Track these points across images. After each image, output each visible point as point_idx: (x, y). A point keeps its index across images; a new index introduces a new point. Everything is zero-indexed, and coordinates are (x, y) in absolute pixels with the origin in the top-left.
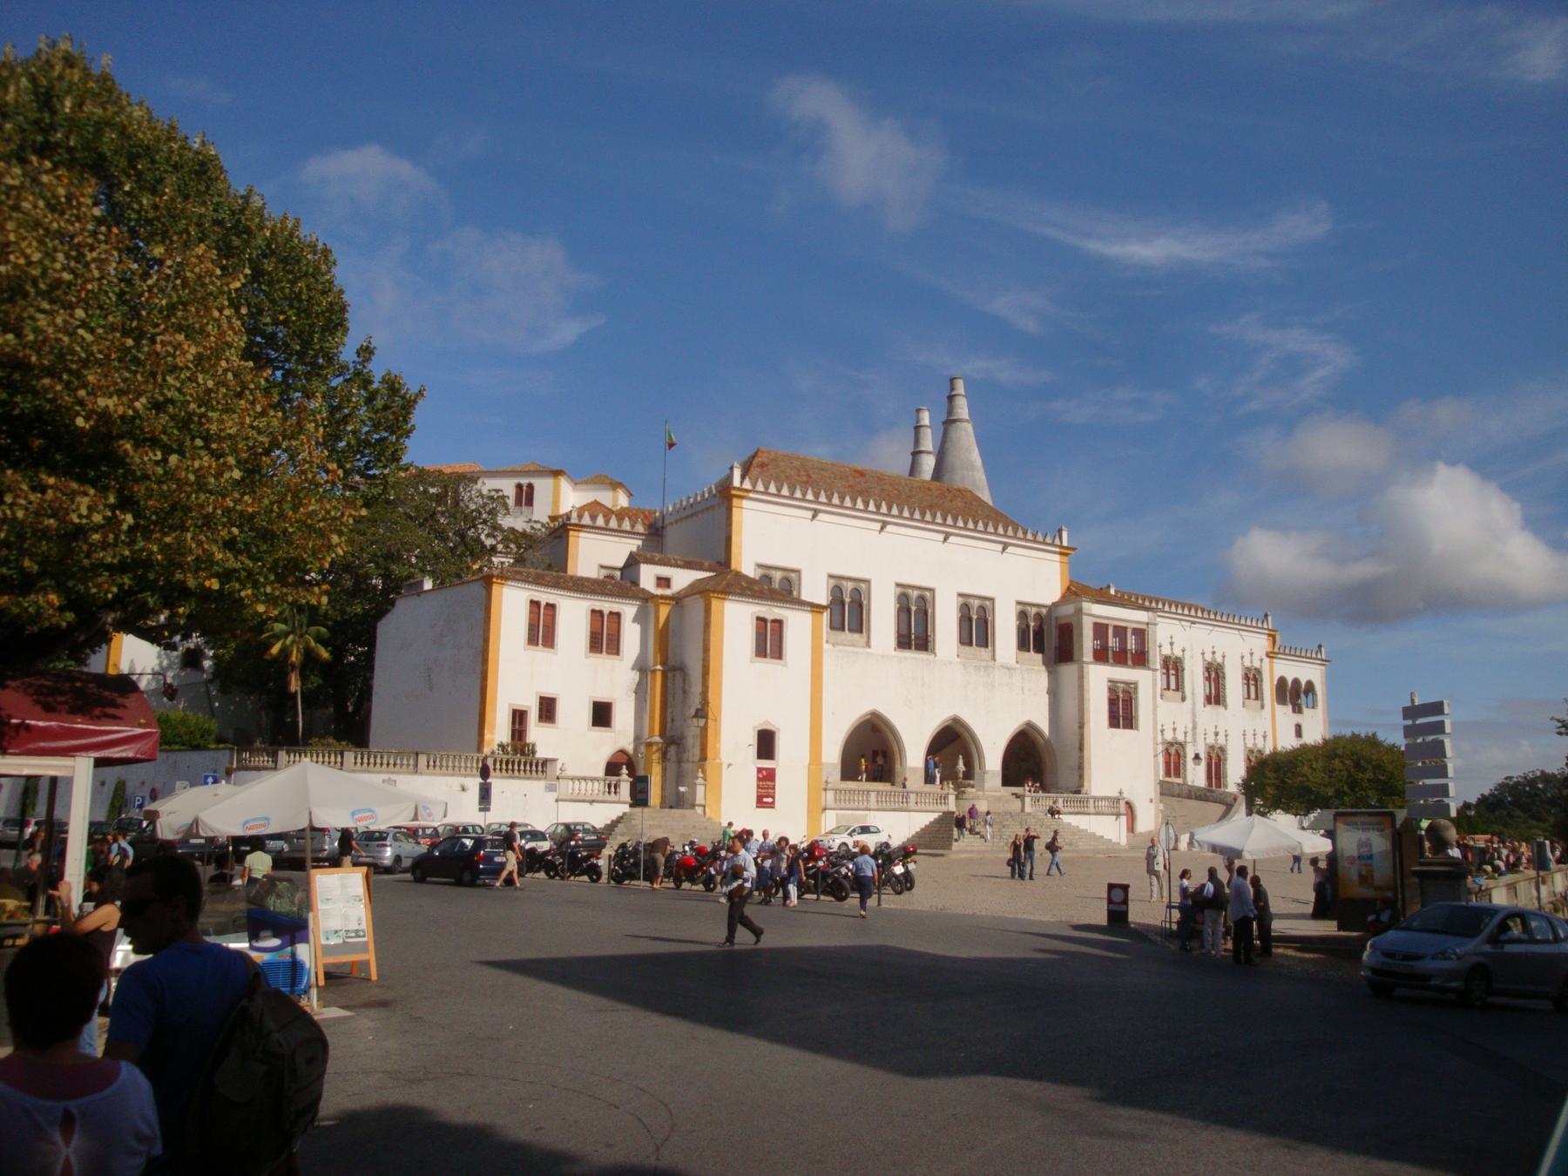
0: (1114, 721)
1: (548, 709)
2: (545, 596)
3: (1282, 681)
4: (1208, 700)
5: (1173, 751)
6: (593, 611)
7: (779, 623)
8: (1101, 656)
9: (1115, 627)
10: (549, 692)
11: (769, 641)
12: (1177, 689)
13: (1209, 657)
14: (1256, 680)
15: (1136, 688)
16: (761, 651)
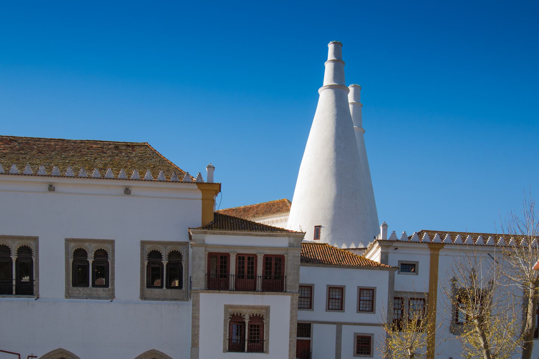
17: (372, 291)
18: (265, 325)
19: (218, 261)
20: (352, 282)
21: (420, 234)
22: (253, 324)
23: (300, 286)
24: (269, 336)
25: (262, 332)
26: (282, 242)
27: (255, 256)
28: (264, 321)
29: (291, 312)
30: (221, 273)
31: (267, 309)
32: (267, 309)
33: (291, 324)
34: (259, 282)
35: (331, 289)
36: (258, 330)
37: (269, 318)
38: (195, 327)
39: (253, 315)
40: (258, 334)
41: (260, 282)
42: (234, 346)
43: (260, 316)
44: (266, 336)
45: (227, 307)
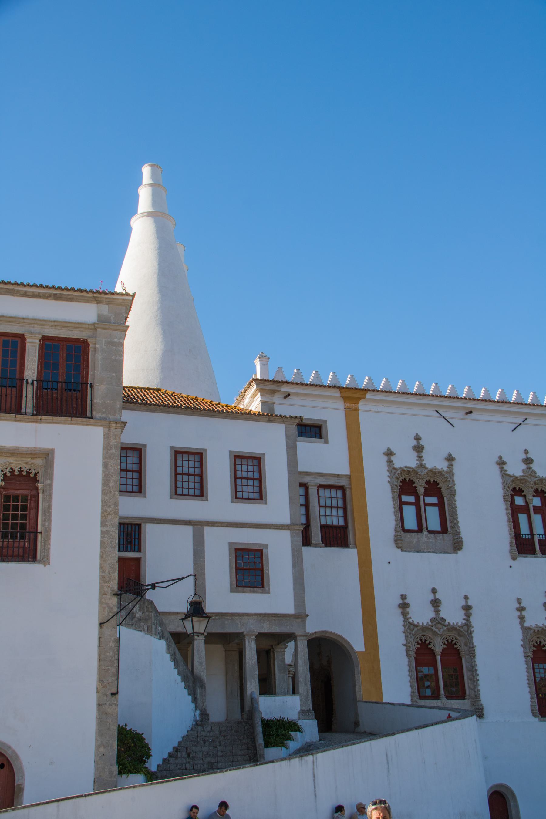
5: (438, 646)
12: (444, 530)
13: (516, 469)
17: (257, 460)
18: (41, 496)
20: (219, 443)
22: (11, 492)
23: (123, 448)
24: (50, 521)
25: (33, 512)
27: (22, 338)
28: (40, 486)
29: (105, 465)
31: (47, 456)
32: (47, 456)
33: (104, 493)
35: (178, 454)
36: (24, 508)
37: (51, 479)
39: (13, 471)
40: (24, 517)
41: (30, 395)
43: (29, 473)
44: (44, 521)
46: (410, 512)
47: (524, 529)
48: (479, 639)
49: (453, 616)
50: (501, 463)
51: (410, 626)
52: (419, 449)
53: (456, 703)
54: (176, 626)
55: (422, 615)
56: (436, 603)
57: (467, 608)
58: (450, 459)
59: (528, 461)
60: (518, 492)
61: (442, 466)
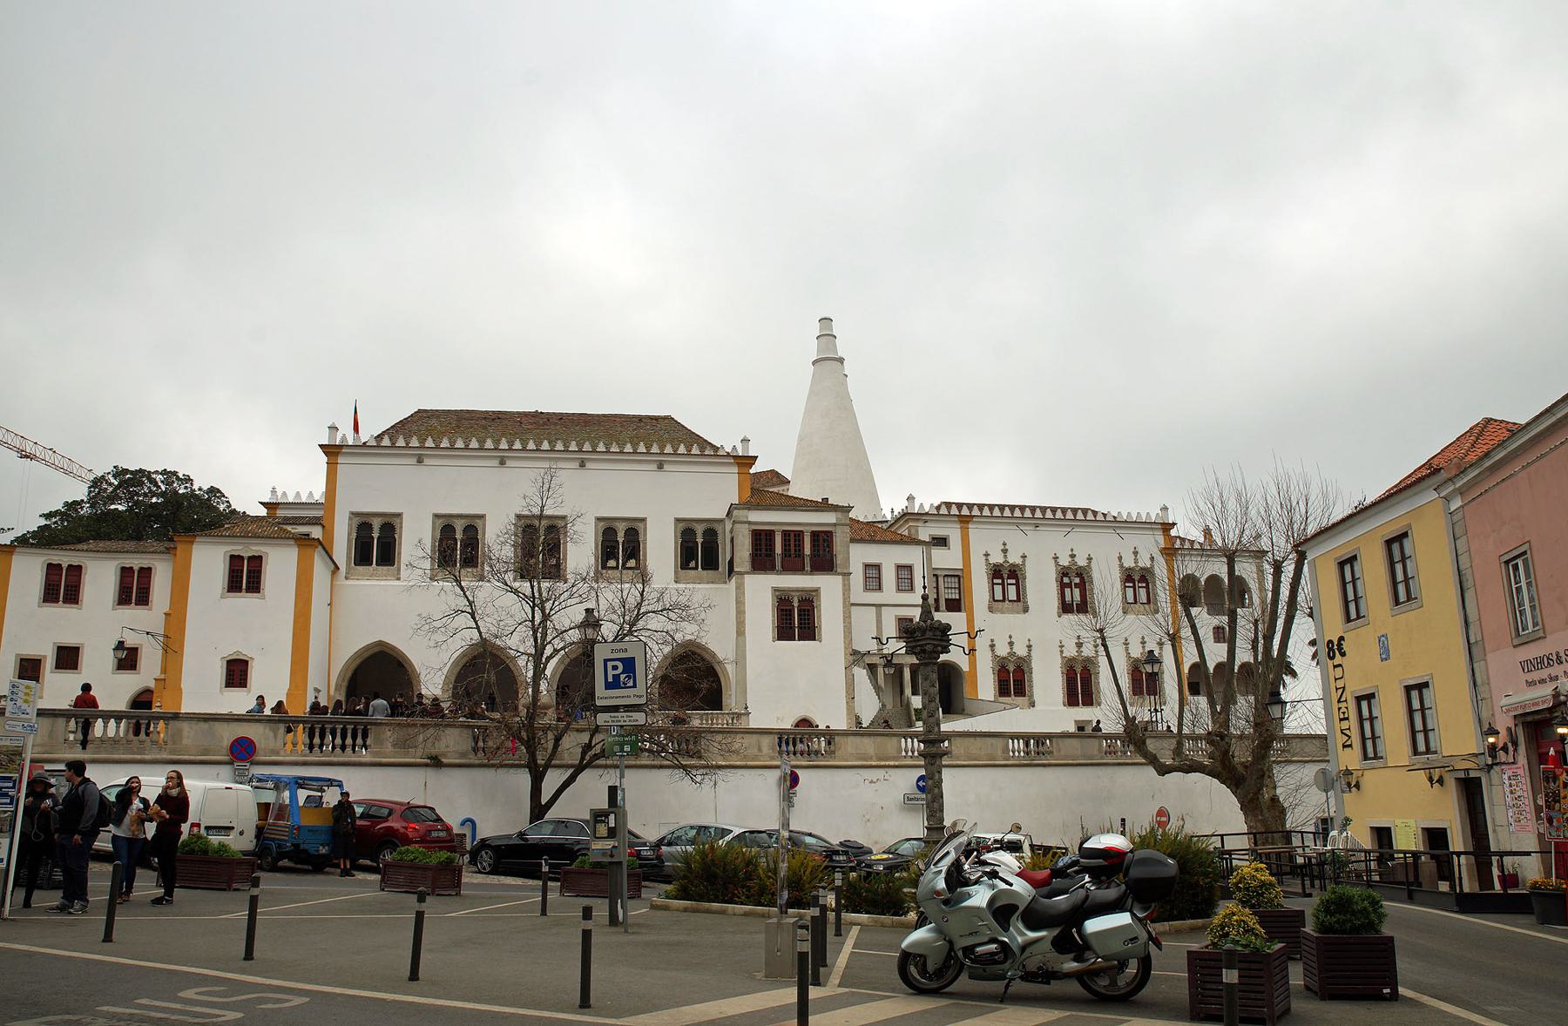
0: (784, 631)
1: (68, 658)
2: (65, 558)
3: (1190, 579)
4: (1066, 608)
5: (1011, 668)
6: (123, 569)
7: (257, 561)
8: (762, 560)
9: (786, 534)
10: (69, 640)
11: (245, 577)
12: (1018, 600)
13: (1065, 561)
14: (1143, 579)
15: (818, 596)
16: (234, 585)
17: (910, 568)
19: (762, 539)
21: (938, 508)
26: (829, 518)
30: (764, 554)
31: (817, 590)
34: (807, 561)
38: (740, 612)
42: (784, 631)
45: (775, 590)
46: (998, 589)
47: (1068, 598)
48: (1036, 665)
49: (1021, 651)
50: (1056, 558)
51: (995, 656)
52: (1005, 551)
53: (1020, 699)
54: (868, 660)
55: (1003, 651)
56: (1011, 644)
57: (1029, 647)
58: (1024, 557)
59: (1073, 556)
60: (1065, 574)
61: (1019, 561)
